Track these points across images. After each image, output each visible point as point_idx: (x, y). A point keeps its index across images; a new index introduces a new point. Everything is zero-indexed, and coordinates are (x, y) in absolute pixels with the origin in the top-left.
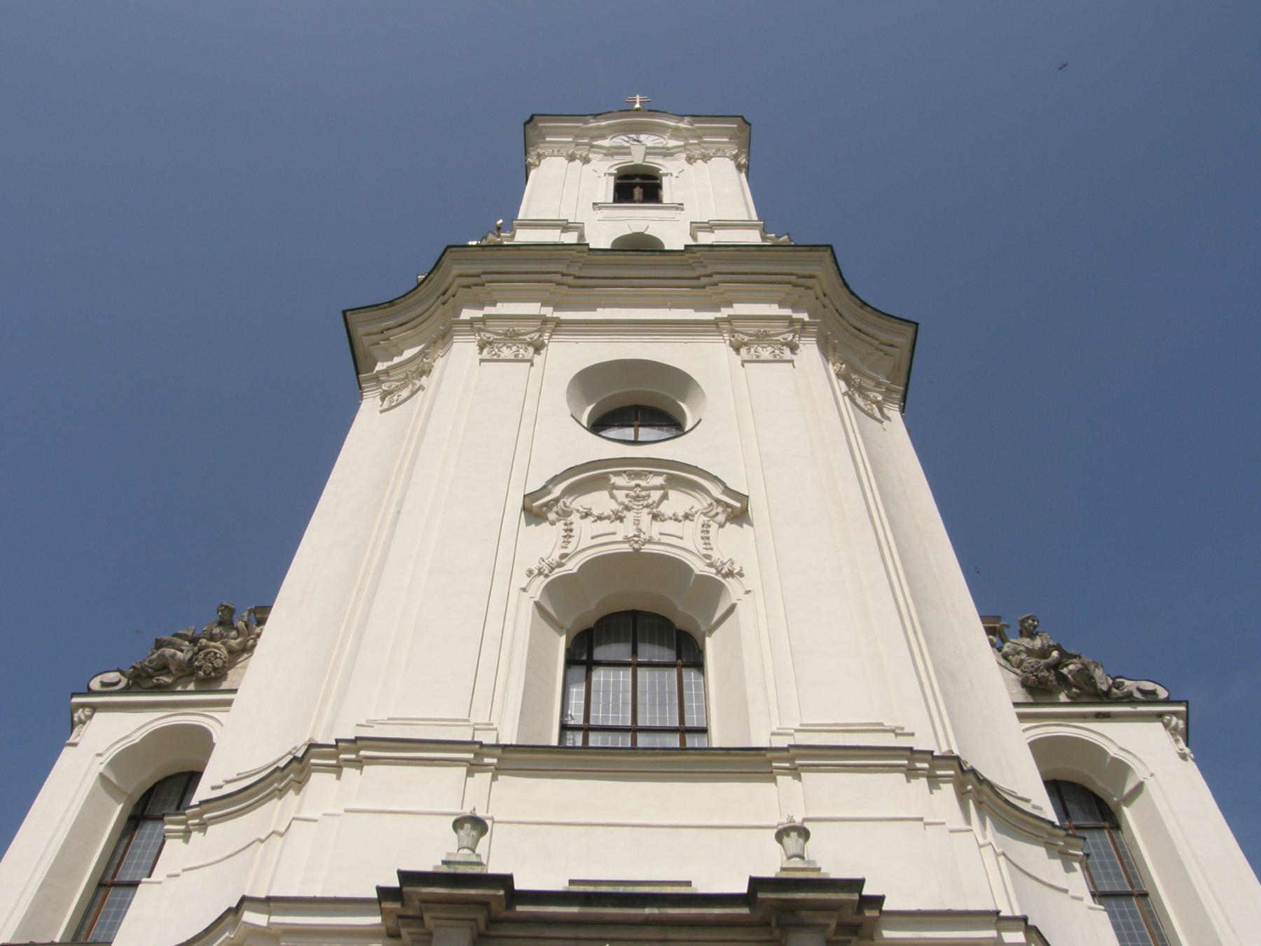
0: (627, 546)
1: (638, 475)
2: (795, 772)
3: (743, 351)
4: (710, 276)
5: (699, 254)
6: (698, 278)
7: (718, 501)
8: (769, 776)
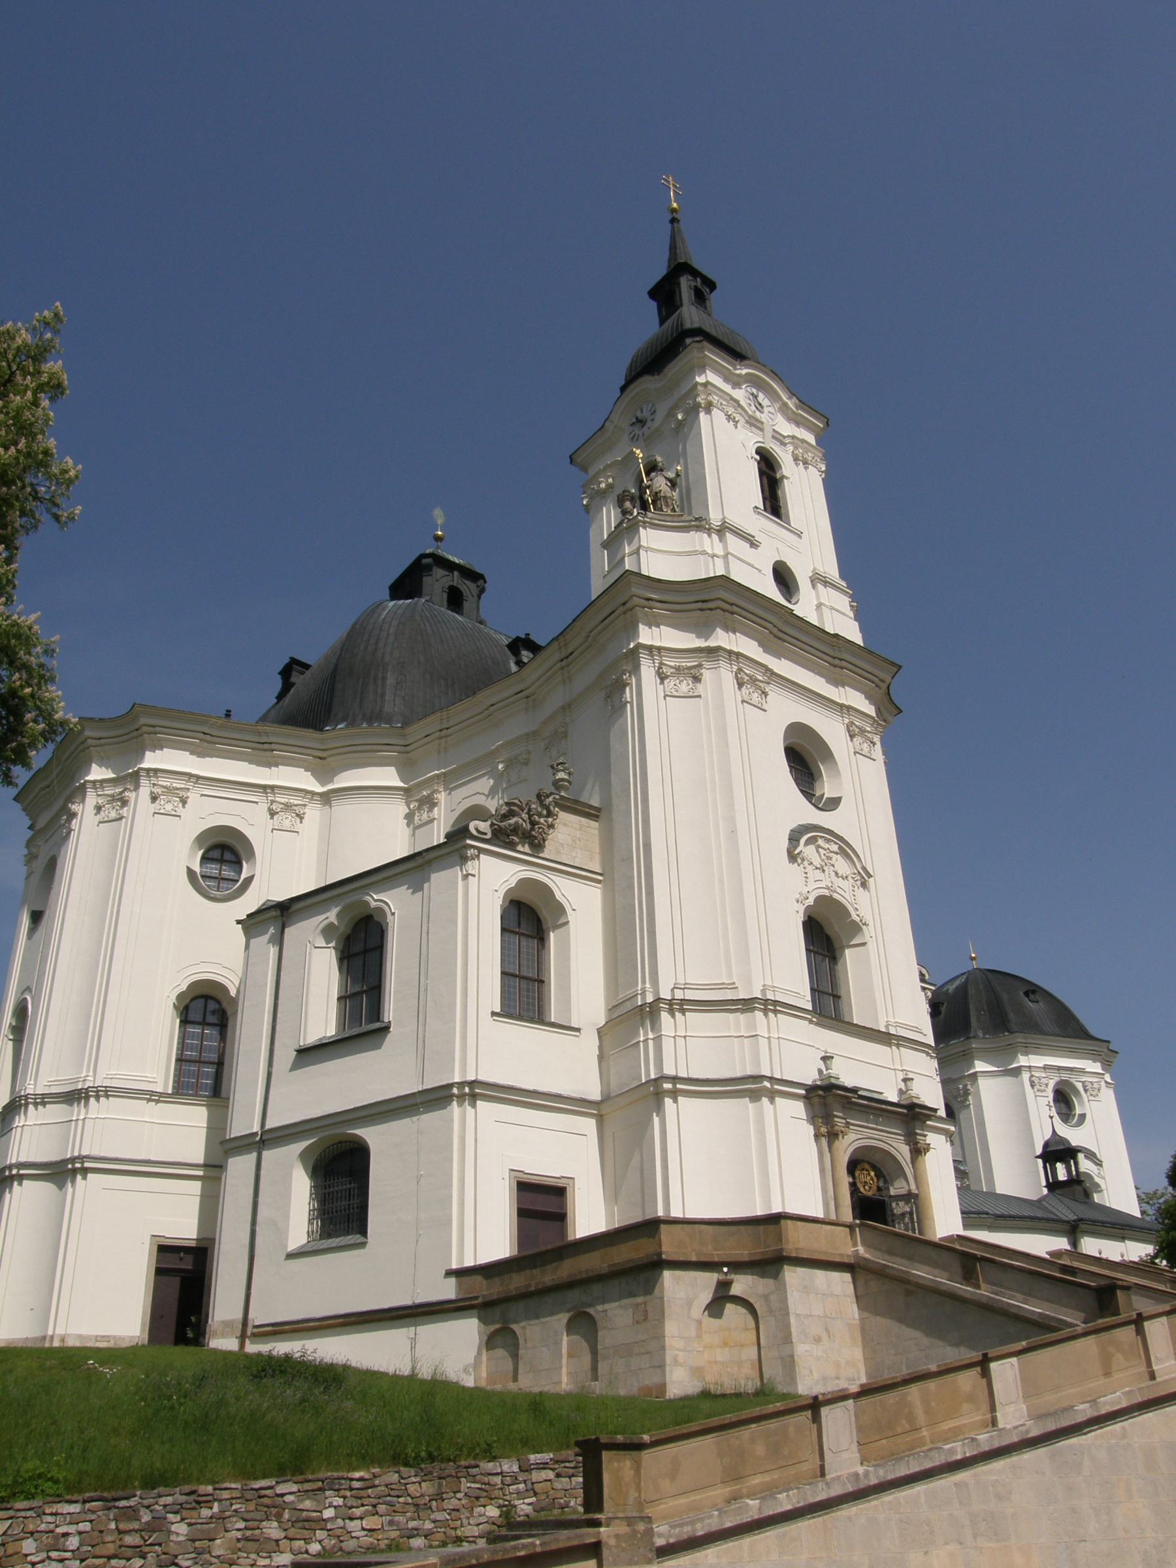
0: (827, 891)
1: (828, 841)
2: (898, 1046)
3: (858, 740)
4: (841, 660)
5: (840, 642)
6: (834, 658)
7: (859, 873)
8: (889, 1044)
